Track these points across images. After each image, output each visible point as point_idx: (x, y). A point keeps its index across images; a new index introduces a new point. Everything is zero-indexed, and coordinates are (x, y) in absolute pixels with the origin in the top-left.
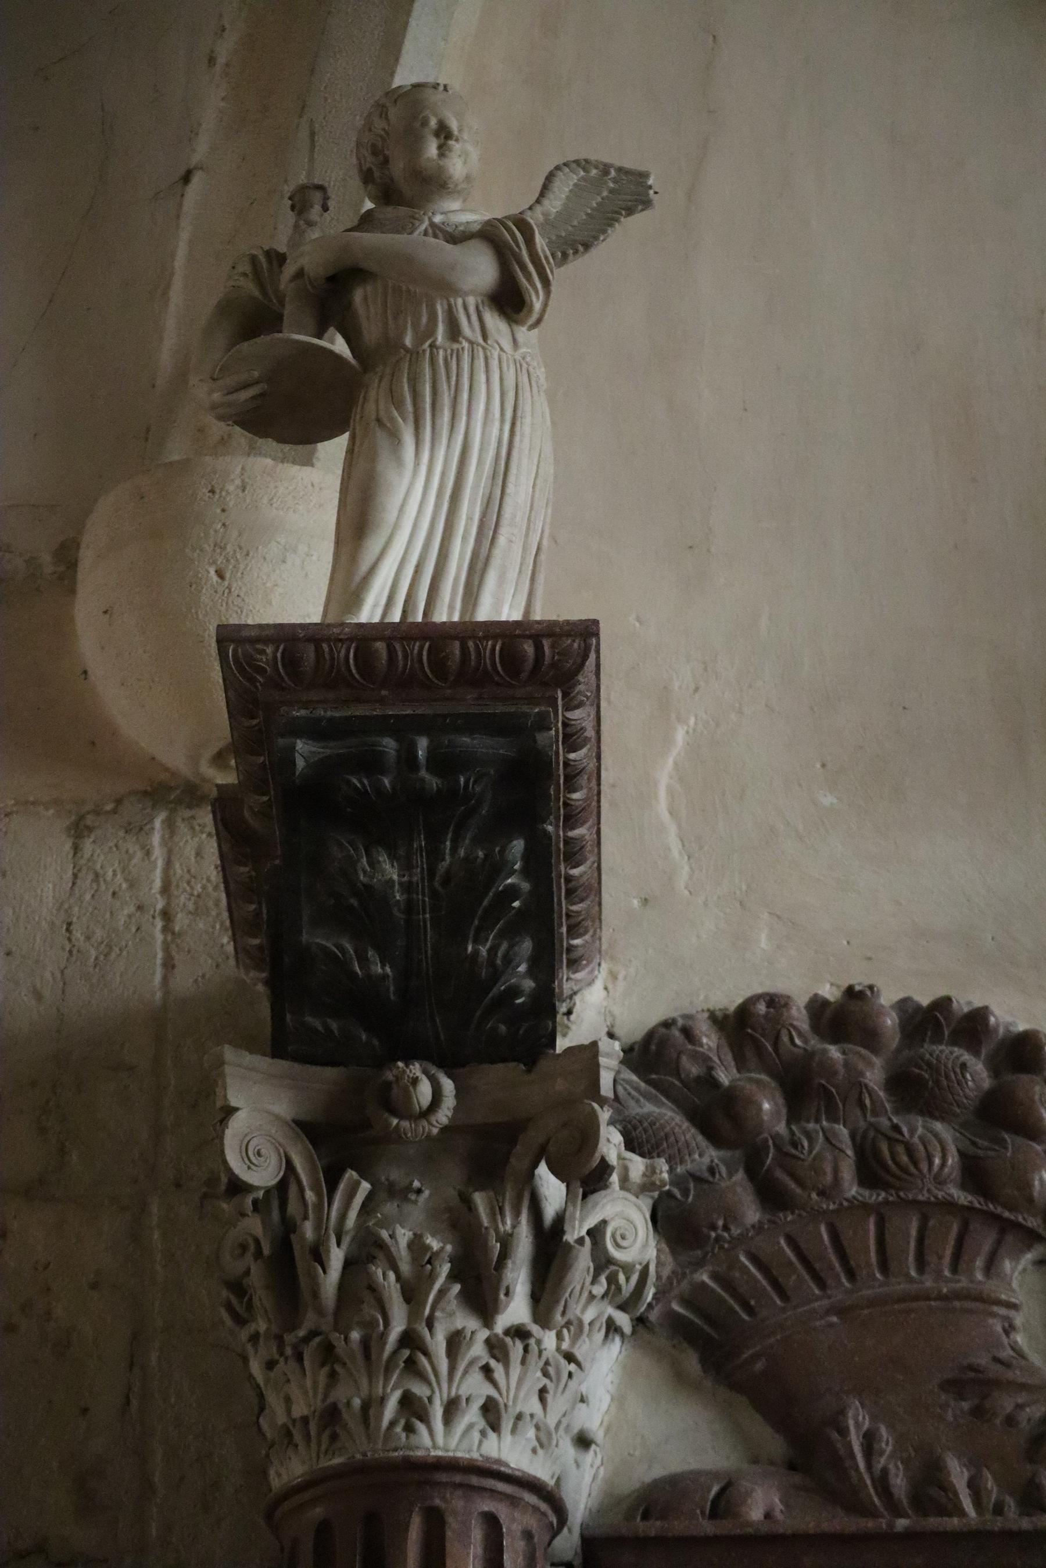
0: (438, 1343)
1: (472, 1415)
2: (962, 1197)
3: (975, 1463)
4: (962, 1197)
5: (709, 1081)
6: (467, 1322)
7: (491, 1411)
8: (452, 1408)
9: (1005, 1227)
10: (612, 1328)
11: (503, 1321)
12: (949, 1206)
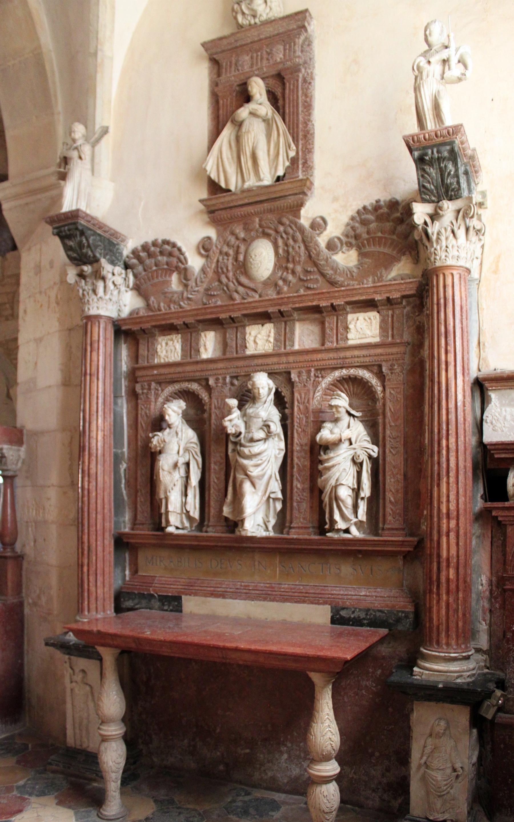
0: (91, 300)
1: (95, 308)
2: (166, 267)
3: (164, 303)
4: (166, 267)
5: (139, 256)
6: (94, 296)
7: (98, 308)
8: (93, 308)
9: (171, 270)
10: (126, 291)
11: (99, 296)
12: (164, 269)
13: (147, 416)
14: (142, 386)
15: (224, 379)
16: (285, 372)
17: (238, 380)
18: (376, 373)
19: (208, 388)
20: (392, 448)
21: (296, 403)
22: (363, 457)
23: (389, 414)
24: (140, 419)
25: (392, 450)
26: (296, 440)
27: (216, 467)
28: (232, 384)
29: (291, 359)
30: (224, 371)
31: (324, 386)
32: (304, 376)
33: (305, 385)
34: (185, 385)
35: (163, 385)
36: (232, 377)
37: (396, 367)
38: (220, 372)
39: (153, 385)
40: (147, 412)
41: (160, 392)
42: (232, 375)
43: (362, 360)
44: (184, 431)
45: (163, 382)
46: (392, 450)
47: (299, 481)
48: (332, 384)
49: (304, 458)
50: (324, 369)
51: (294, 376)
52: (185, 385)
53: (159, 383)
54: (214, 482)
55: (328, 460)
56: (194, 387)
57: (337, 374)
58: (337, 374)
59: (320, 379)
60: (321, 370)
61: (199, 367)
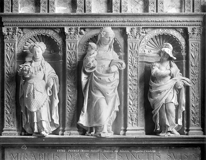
13: (12, 51)
14: (8, 29)
15: (77, 29)
16: (120, 28)
17: (85, 30)
18: (182, 33)
19: (63, 35)
20: (193, 80)
21: (129, 49)
22: (181, 85)
23: (191, 59)
24: (6, 53)
25: (193, 81)
26: (129, 73)
27: (70, 90)
28: (81, 33)
29: (126, 19)
30: (75, 23)
31: (146, 39)
32: (135, 31)
33: (135, 37)
34: (43, 32)
35: (25, 30)
36: (80, 28)
37: (195, 30)
38: (74, 24)
39: (17, 30)
40: (12, 49)
41: (22, 35)
42: (81, 27)
43: (174, 23)
44: (46, 64)
45: (25, 28)
46: (193, 81)
47: (131, 100)
48: (152, 39)
49: (135, 85)
50: (147, 28)
51: (128, 30)
52: (43, 32)
53: (22, 29)
54: (68, 100)
55: (158, 87)
56: (51, 33)
57: (161, 31)
58: (156, 32)
59: (144, 34)
60: (144, 28)
61: (56, 19)
